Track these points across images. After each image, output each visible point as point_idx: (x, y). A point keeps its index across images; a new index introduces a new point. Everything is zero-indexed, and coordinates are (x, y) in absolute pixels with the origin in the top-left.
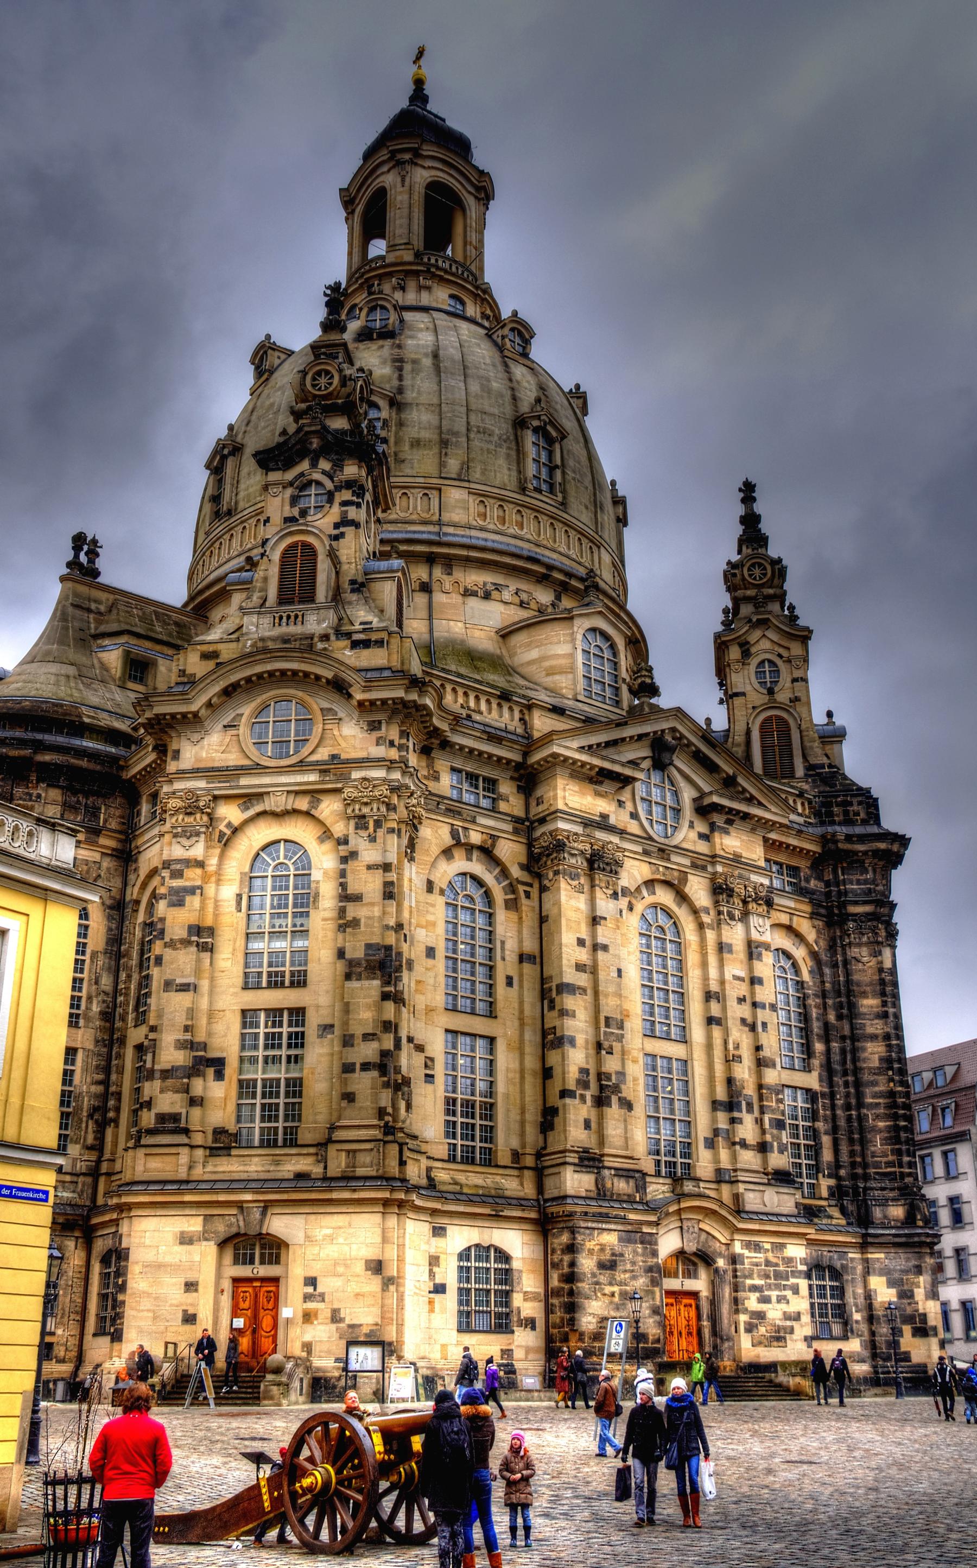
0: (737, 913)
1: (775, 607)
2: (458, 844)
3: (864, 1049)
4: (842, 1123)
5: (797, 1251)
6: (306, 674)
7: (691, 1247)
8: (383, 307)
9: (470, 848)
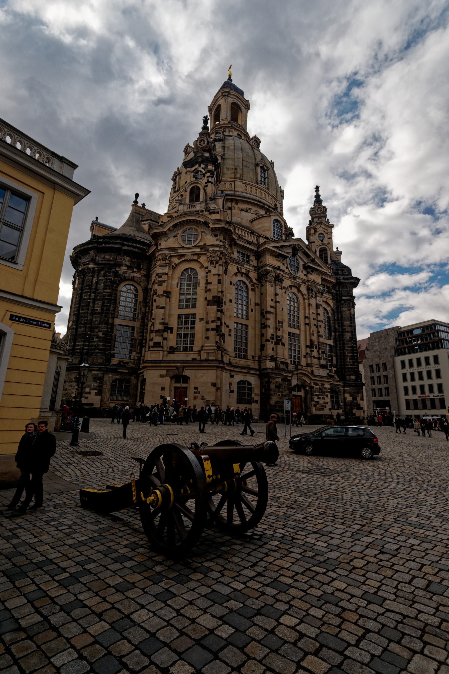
1: (324, 219)
2: (239, 272)
4: (339, 354)
5: (327, 386)
6: (197, 221)
7: (300, 384)
8: (220, 133)
9: (242, 274)
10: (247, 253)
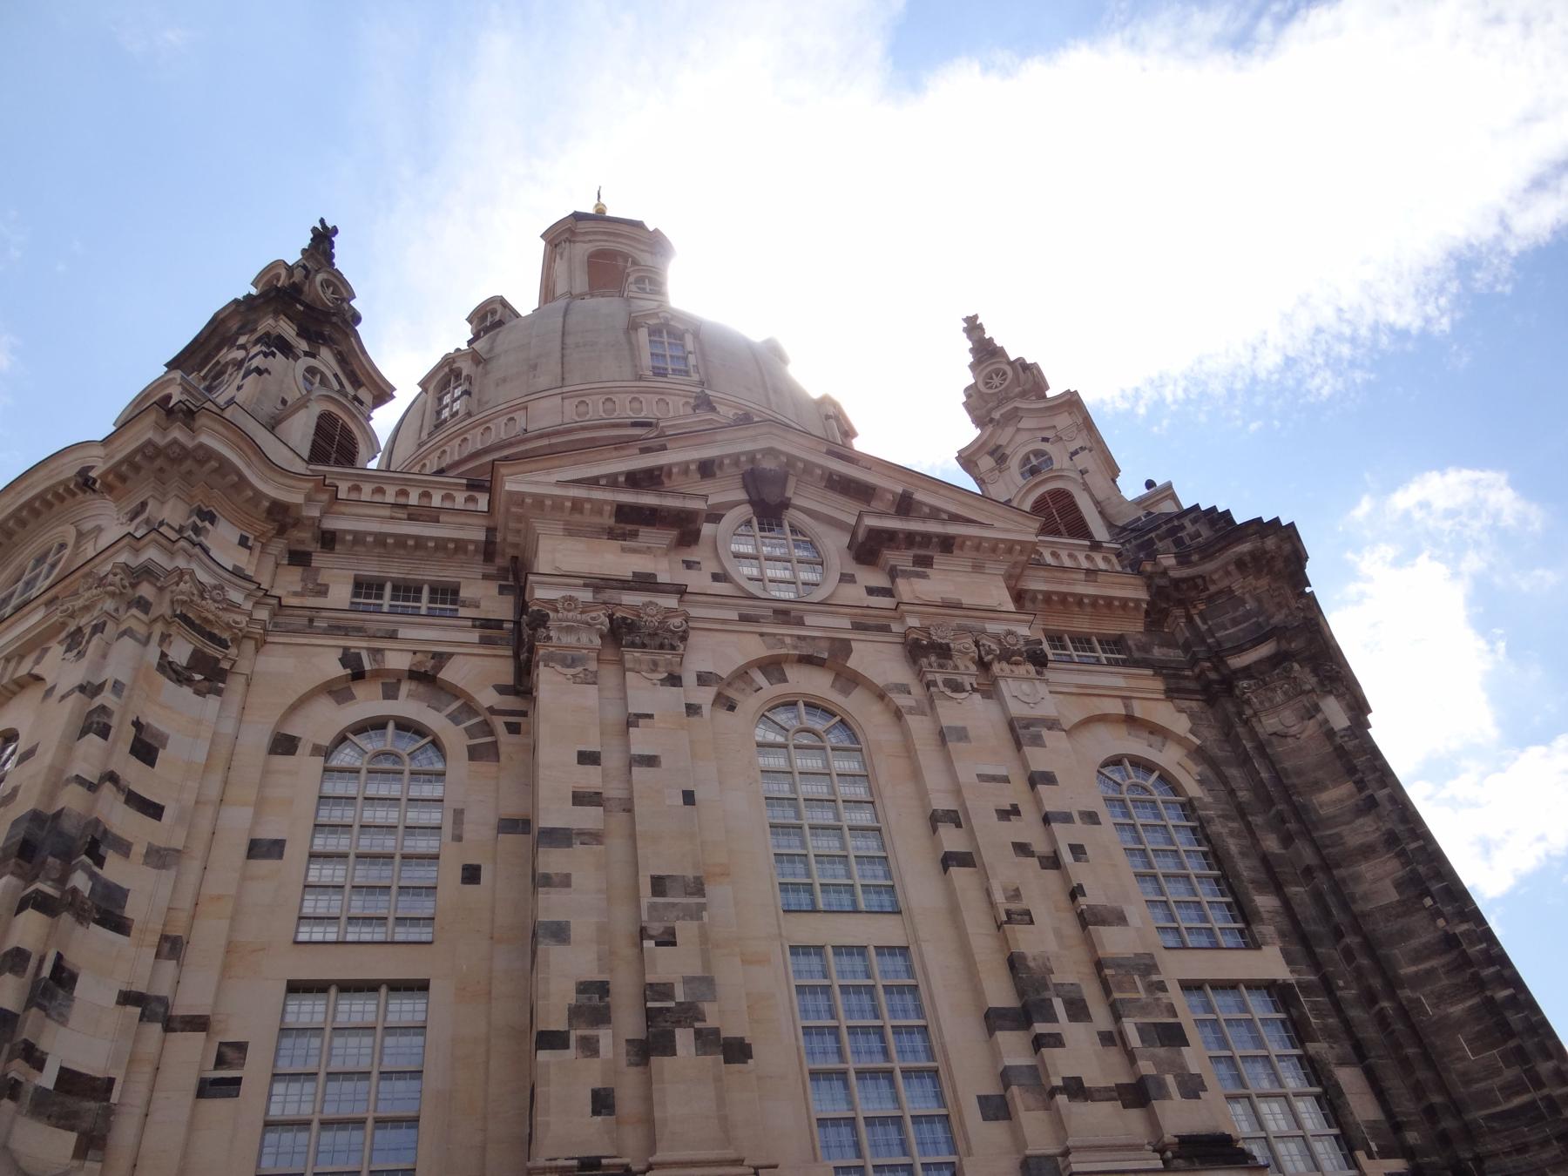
0: (967, 681)
2: (359, 675)
3: (1357, 878)
4: (1370, 1033)
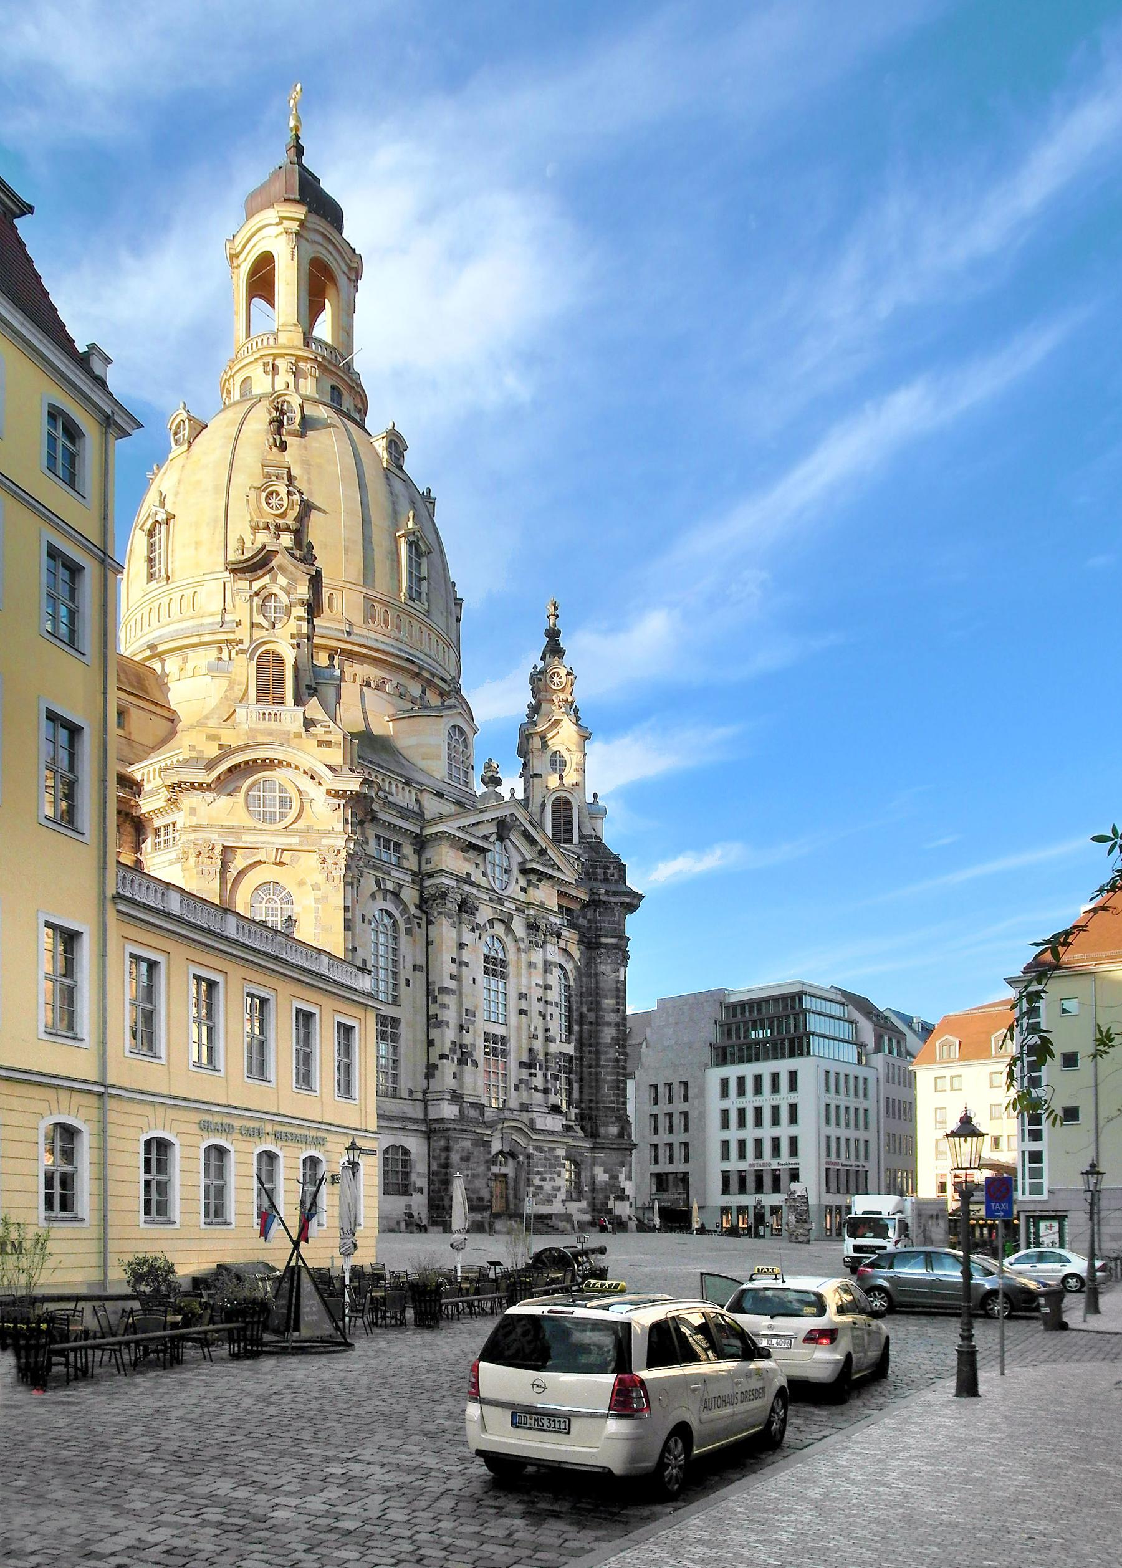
3: (602, 1031)
4: (585, 1075)
5: (561, 1152)
7: (506, 1150)
10: (396, 838)
